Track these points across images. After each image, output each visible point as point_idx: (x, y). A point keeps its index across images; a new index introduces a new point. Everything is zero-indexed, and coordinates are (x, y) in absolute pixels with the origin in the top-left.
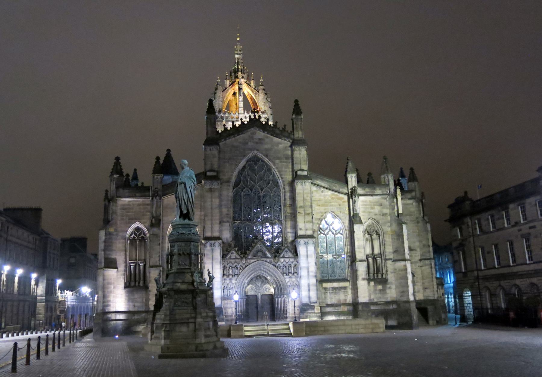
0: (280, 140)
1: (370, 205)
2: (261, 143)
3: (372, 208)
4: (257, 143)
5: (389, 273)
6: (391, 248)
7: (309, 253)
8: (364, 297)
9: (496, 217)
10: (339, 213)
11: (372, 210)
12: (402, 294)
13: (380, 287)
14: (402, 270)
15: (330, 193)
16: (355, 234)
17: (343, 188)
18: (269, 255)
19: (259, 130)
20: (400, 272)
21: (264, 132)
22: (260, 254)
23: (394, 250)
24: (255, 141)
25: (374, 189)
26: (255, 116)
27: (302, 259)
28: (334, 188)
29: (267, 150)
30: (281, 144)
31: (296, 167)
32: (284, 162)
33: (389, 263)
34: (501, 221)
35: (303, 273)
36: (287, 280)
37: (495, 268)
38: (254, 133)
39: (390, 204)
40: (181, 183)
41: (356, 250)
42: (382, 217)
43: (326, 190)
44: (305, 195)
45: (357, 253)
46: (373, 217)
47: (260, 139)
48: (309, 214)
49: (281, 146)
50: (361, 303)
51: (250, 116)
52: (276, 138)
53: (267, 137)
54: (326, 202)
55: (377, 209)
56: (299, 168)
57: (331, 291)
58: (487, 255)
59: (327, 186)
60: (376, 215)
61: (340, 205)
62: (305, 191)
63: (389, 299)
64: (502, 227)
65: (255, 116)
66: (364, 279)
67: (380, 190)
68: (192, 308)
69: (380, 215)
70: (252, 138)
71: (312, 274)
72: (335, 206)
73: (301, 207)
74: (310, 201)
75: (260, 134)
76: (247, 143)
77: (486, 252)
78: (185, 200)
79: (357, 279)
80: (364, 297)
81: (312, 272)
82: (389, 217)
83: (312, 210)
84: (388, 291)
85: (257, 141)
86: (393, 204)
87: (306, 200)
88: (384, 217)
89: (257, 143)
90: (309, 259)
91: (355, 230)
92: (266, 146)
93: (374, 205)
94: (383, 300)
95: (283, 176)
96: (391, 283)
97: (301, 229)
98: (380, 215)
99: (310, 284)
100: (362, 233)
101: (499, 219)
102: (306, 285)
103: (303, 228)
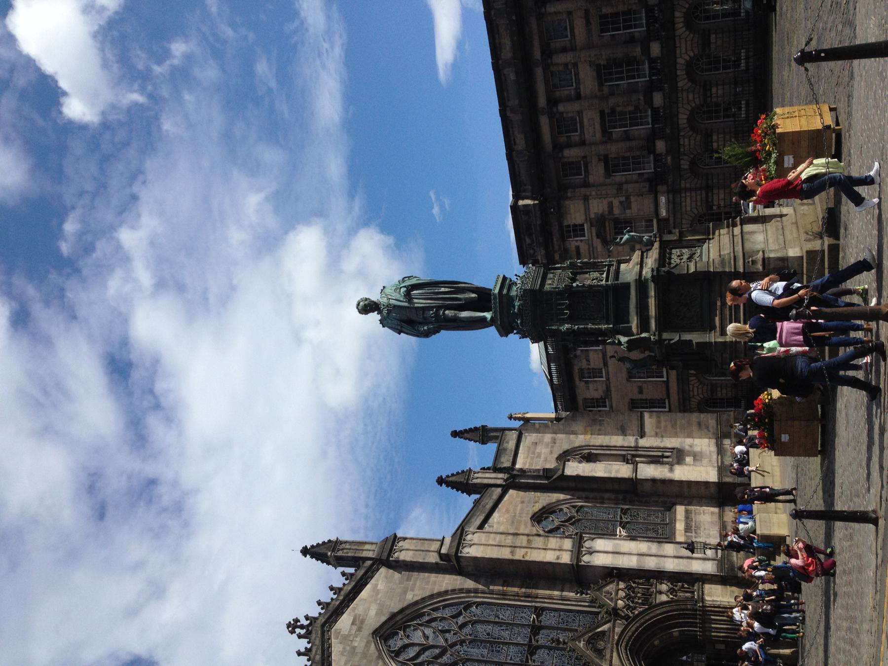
0: (369, 586)
1: (532, 458)
2: (362, 622)
3: (539, 456)
4: (359, 629)
5: (662, 445)
6: (615, 437)
7: (610, 549)
8: (707, 473)
9: (584, 365)
10: (537, 505)
11: (543, 456)
12: (703, 426)
13: (688, 459)
14: (659, 422)
15: (496, 515)
16: (582, 474)
17: (491, 495)
18: (605, 627)
19: (336, 622)
20: (663, 424)
21: (343, 613)
22: (601, 644)
23: (620, 432)
24: (353, 632)
25: (505, 450)
26: (302, 627)
27: (620, 563)
28: (489, 506)
29: (379, 613)
30: (376, 585)
31: (433, 558)
32: (414, 584)
33: (643, 442)
34: (591, 355)
35: (651, 564)
36: (664, 598)
37: (667, 383)
38: (338, 633)
39: (537, 431)
40: (408, 295)
41: (612, 475)
42: (557, 445)
43: (491, 520)
44: (491, 542)
45: (620, 475)
46: (556, 456)
47: (353, 624)
48: (529, 541)
49: (380, 587)
50: (719, 478)
51: (300, 636)
52: (363, 593)
53: (355, 608)
54: (513, 522)
55: (543, 450)
56: (436, 555)
57: (693, 534)
58: (644, 397)
59: (482, 518)
60: (551, 452)
61: (523, 502)
62: (483, 542)
63: (713, 449)
64: (601, 355)
65: (302, 627)
66: (671, 470)
67: (508, 442)
68: (705, 246)
69: (552, 447)
70: (345, 639)
71: (654, 548)
72: (522, 509)
73: (512, 553)
74: (503, 536)
75: (344, 622)
76: (354, 648)
77: (640, 397)
78: (447, 290)
79: (671, 482)
80: (707, 473)
81: (649, 548)
82: (559, 435)
83: (523, 535)
84: (697, 449)
85: (355, 628)
86: (537, 426)
87: (500, 541)
88: (558, 441)
89: (359, 629)
90: (622, 550)
91: (574, 474)
92: (372, 612)
93: (534, 453)
94: (715, 457)
95: (443, 589)
96: (681, 443)
97: (558, 558)
98: (552, 447)
99: (676, 554)
100: (581, 465)
101: (588, 360)
102: (676, 560)
103: (558, 553)
